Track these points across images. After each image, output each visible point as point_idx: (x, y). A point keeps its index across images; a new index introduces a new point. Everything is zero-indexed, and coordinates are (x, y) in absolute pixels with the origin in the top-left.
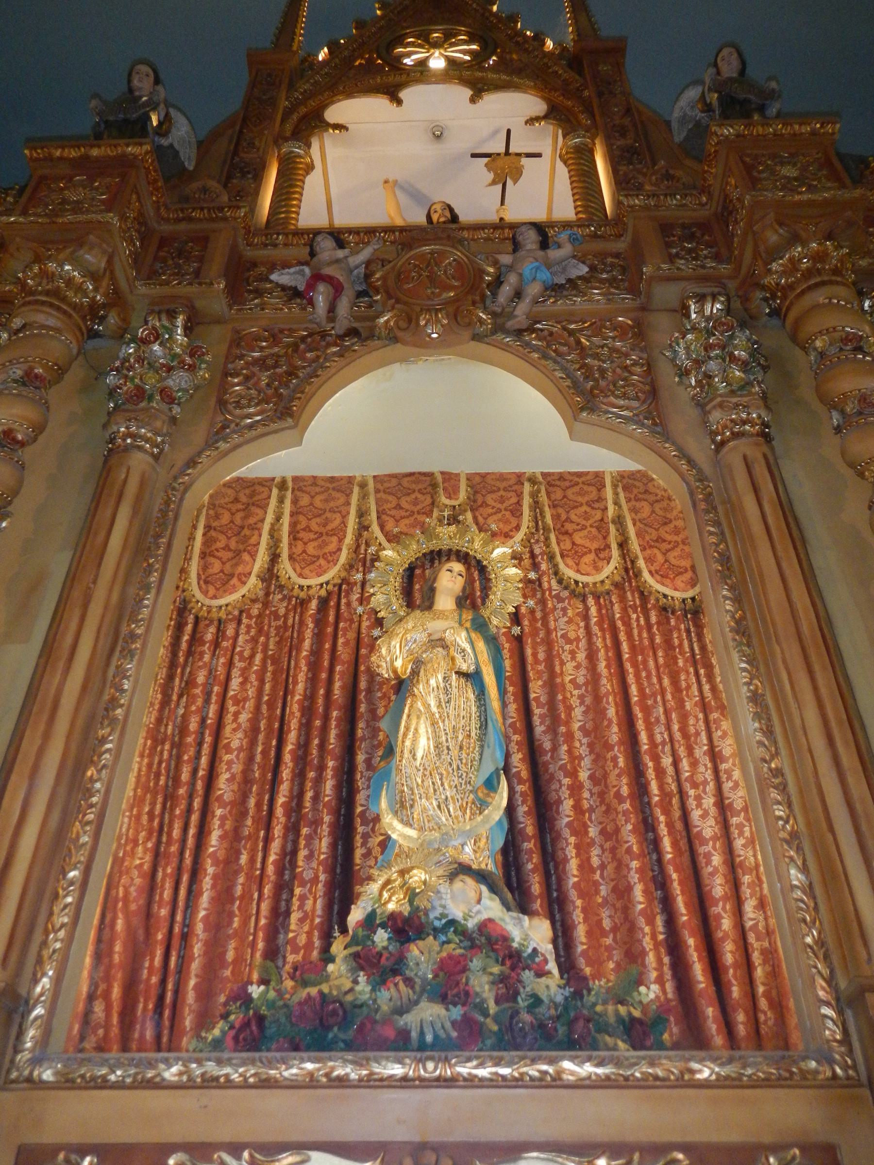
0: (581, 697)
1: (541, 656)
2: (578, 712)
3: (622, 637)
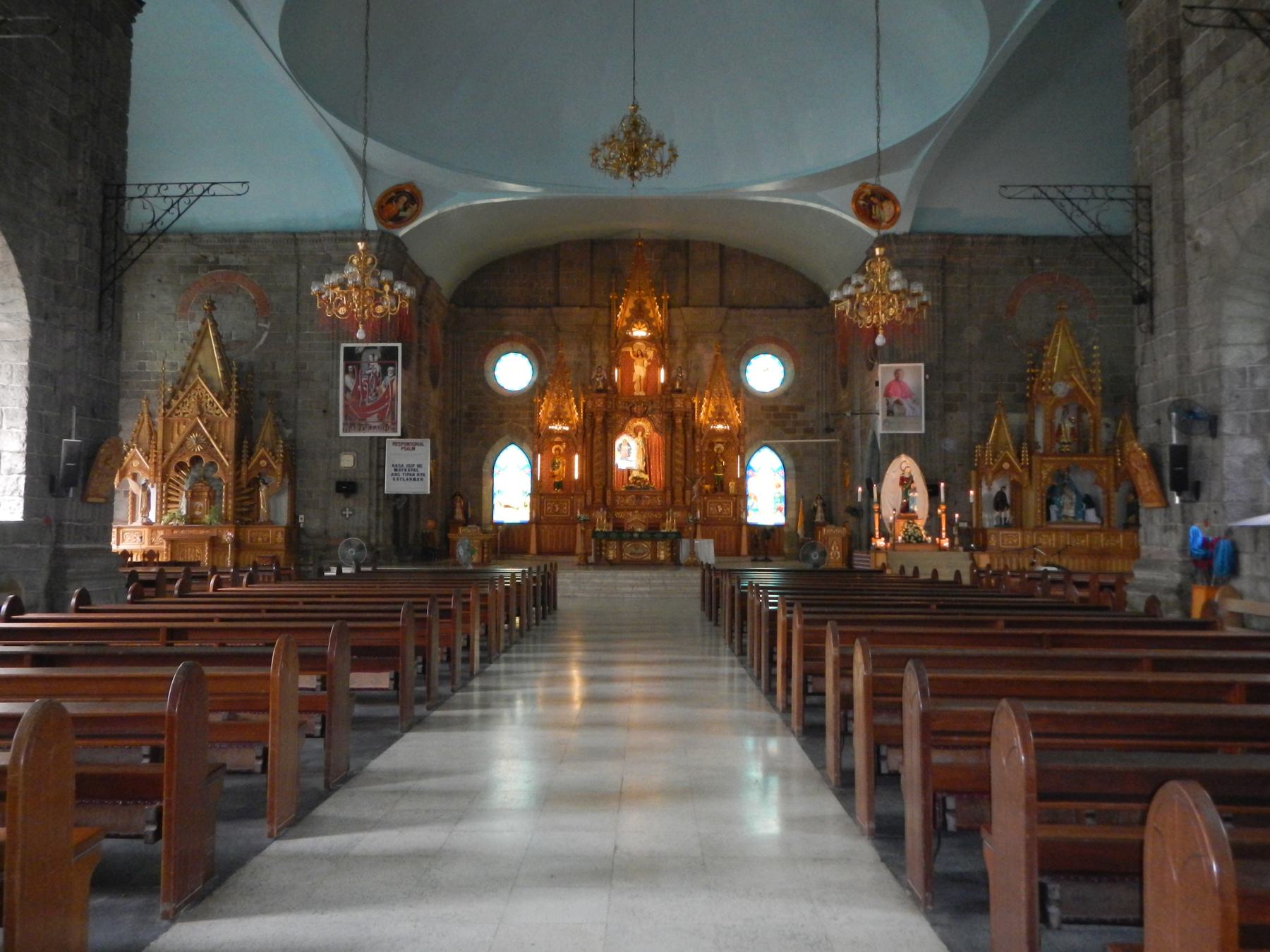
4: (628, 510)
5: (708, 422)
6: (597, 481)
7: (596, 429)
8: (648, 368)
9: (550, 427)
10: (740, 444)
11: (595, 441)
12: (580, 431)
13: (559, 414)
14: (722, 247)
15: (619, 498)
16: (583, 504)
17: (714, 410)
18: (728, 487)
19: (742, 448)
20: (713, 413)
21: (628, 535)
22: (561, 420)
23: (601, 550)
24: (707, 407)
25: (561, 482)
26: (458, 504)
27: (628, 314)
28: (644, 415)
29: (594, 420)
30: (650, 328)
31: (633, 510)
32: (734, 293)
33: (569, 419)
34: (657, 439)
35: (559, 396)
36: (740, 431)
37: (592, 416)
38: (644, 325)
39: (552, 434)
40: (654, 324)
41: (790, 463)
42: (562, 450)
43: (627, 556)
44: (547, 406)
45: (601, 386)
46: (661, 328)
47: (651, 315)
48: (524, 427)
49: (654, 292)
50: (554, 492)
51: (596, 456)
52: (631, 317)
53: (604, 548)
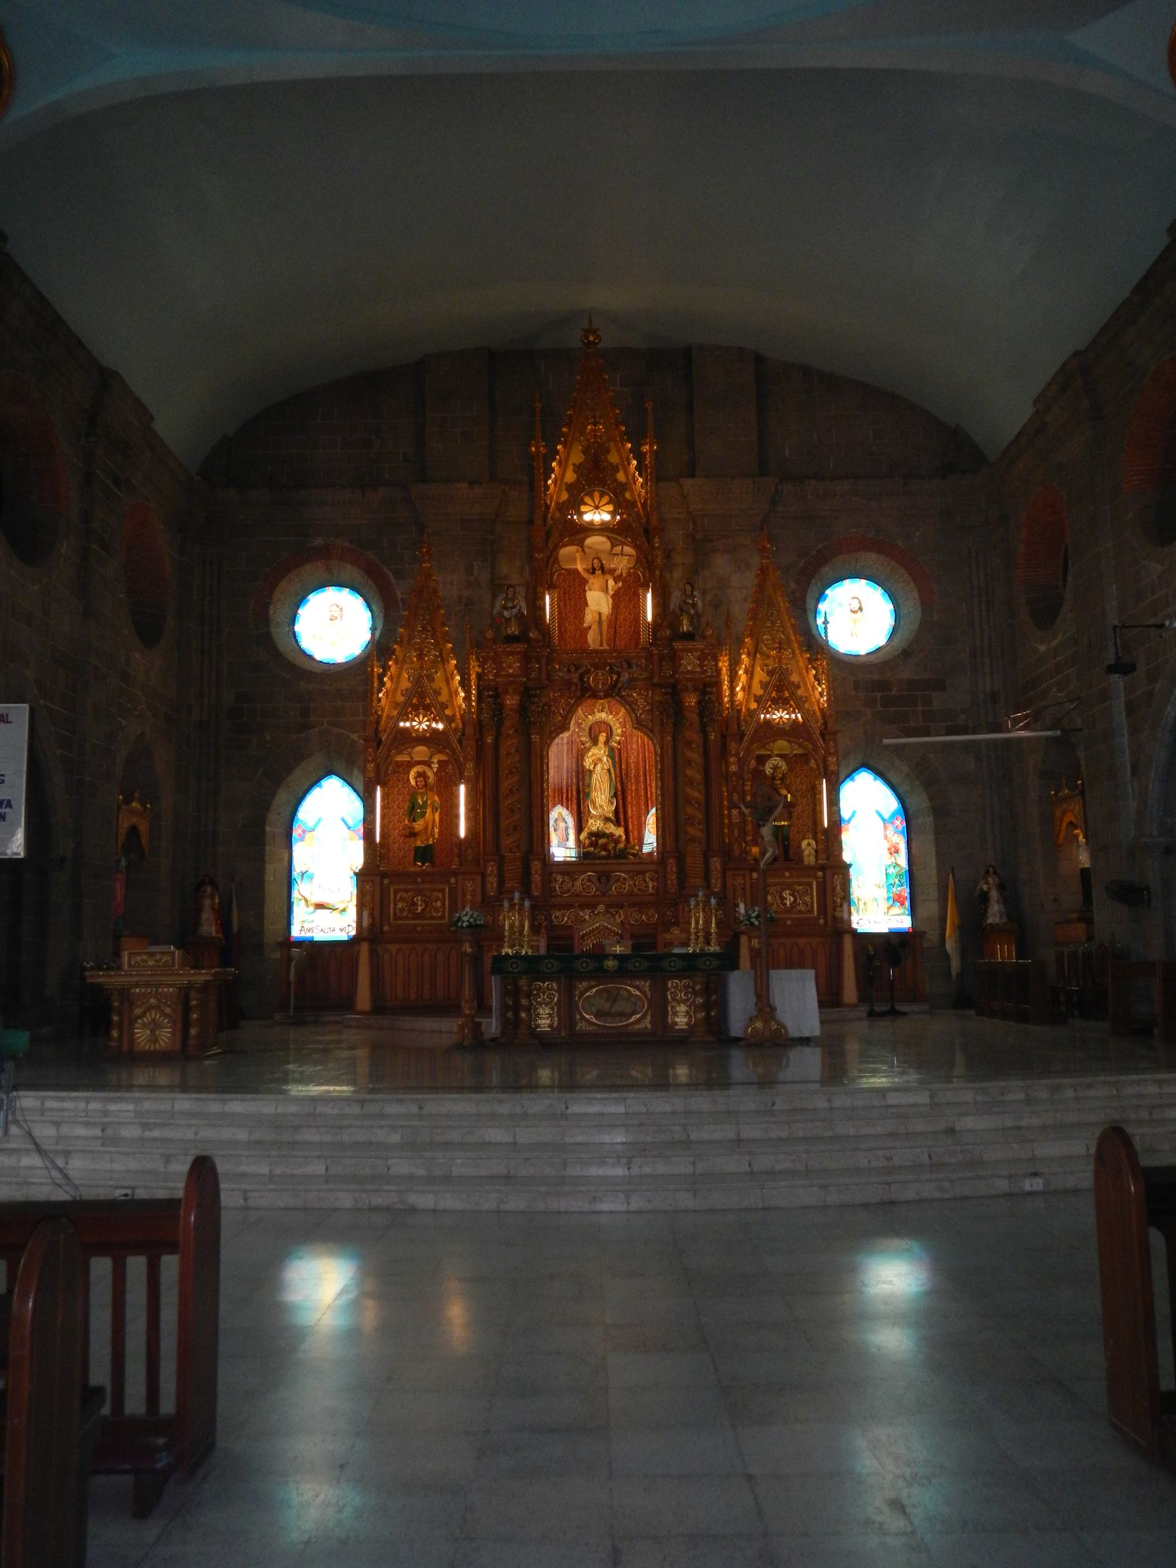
0: (635, 767)
1: (625, 755)
2: (633, 771)
3: (646, 749)
4: (583, 906)
5: (754, 706)
6: (507, 841)
7: (507, 723)
8: (616, 597)
9: (402, 724)
10: (827, 751)
11: (503, 752)
12: (470, 731)
13: (422, 696)
14: (759, 359)
15: (559, 878)
16: (479, 898)
17: (766, 678)
18: (800, 852)
19: (832, 759)
20: (764, 686)
21: (592, 965)
22: (427, 708)
23: (517, 1007)
24: (750, 673)
25: (428, 847)
26: (207, 902)
27: (570, 477)
28: (613, 692)
29: (502, 706)
30: (619, 505)
31: (592, 906)
32: (787, 453)
33: (444, 706)
34: (642, 747)
35: (421, 657)
36: (825, 723)
37: (497, 696)
38: (606, 499)
39: (408, 739)
40: (628, 495)
41: (920, 801)
42: (432, 779)
43: (588, 1020)
44: (396, 679)
45: (513, 629)
46: (644, 505)
47: (621, 477)
48: (355, 737)
49: (625, 433)
50: (413, 869)
51: (505, 786)
52: (578, 481)
53: (524, 1002)
